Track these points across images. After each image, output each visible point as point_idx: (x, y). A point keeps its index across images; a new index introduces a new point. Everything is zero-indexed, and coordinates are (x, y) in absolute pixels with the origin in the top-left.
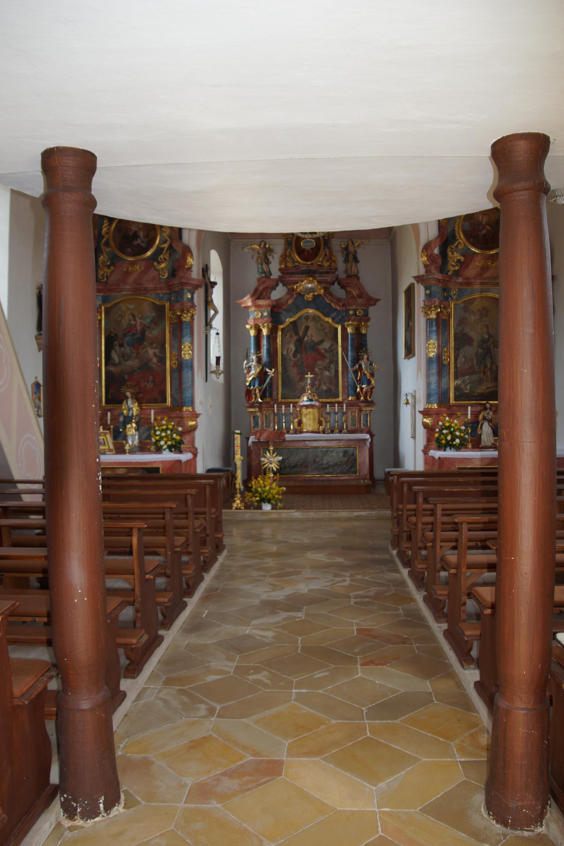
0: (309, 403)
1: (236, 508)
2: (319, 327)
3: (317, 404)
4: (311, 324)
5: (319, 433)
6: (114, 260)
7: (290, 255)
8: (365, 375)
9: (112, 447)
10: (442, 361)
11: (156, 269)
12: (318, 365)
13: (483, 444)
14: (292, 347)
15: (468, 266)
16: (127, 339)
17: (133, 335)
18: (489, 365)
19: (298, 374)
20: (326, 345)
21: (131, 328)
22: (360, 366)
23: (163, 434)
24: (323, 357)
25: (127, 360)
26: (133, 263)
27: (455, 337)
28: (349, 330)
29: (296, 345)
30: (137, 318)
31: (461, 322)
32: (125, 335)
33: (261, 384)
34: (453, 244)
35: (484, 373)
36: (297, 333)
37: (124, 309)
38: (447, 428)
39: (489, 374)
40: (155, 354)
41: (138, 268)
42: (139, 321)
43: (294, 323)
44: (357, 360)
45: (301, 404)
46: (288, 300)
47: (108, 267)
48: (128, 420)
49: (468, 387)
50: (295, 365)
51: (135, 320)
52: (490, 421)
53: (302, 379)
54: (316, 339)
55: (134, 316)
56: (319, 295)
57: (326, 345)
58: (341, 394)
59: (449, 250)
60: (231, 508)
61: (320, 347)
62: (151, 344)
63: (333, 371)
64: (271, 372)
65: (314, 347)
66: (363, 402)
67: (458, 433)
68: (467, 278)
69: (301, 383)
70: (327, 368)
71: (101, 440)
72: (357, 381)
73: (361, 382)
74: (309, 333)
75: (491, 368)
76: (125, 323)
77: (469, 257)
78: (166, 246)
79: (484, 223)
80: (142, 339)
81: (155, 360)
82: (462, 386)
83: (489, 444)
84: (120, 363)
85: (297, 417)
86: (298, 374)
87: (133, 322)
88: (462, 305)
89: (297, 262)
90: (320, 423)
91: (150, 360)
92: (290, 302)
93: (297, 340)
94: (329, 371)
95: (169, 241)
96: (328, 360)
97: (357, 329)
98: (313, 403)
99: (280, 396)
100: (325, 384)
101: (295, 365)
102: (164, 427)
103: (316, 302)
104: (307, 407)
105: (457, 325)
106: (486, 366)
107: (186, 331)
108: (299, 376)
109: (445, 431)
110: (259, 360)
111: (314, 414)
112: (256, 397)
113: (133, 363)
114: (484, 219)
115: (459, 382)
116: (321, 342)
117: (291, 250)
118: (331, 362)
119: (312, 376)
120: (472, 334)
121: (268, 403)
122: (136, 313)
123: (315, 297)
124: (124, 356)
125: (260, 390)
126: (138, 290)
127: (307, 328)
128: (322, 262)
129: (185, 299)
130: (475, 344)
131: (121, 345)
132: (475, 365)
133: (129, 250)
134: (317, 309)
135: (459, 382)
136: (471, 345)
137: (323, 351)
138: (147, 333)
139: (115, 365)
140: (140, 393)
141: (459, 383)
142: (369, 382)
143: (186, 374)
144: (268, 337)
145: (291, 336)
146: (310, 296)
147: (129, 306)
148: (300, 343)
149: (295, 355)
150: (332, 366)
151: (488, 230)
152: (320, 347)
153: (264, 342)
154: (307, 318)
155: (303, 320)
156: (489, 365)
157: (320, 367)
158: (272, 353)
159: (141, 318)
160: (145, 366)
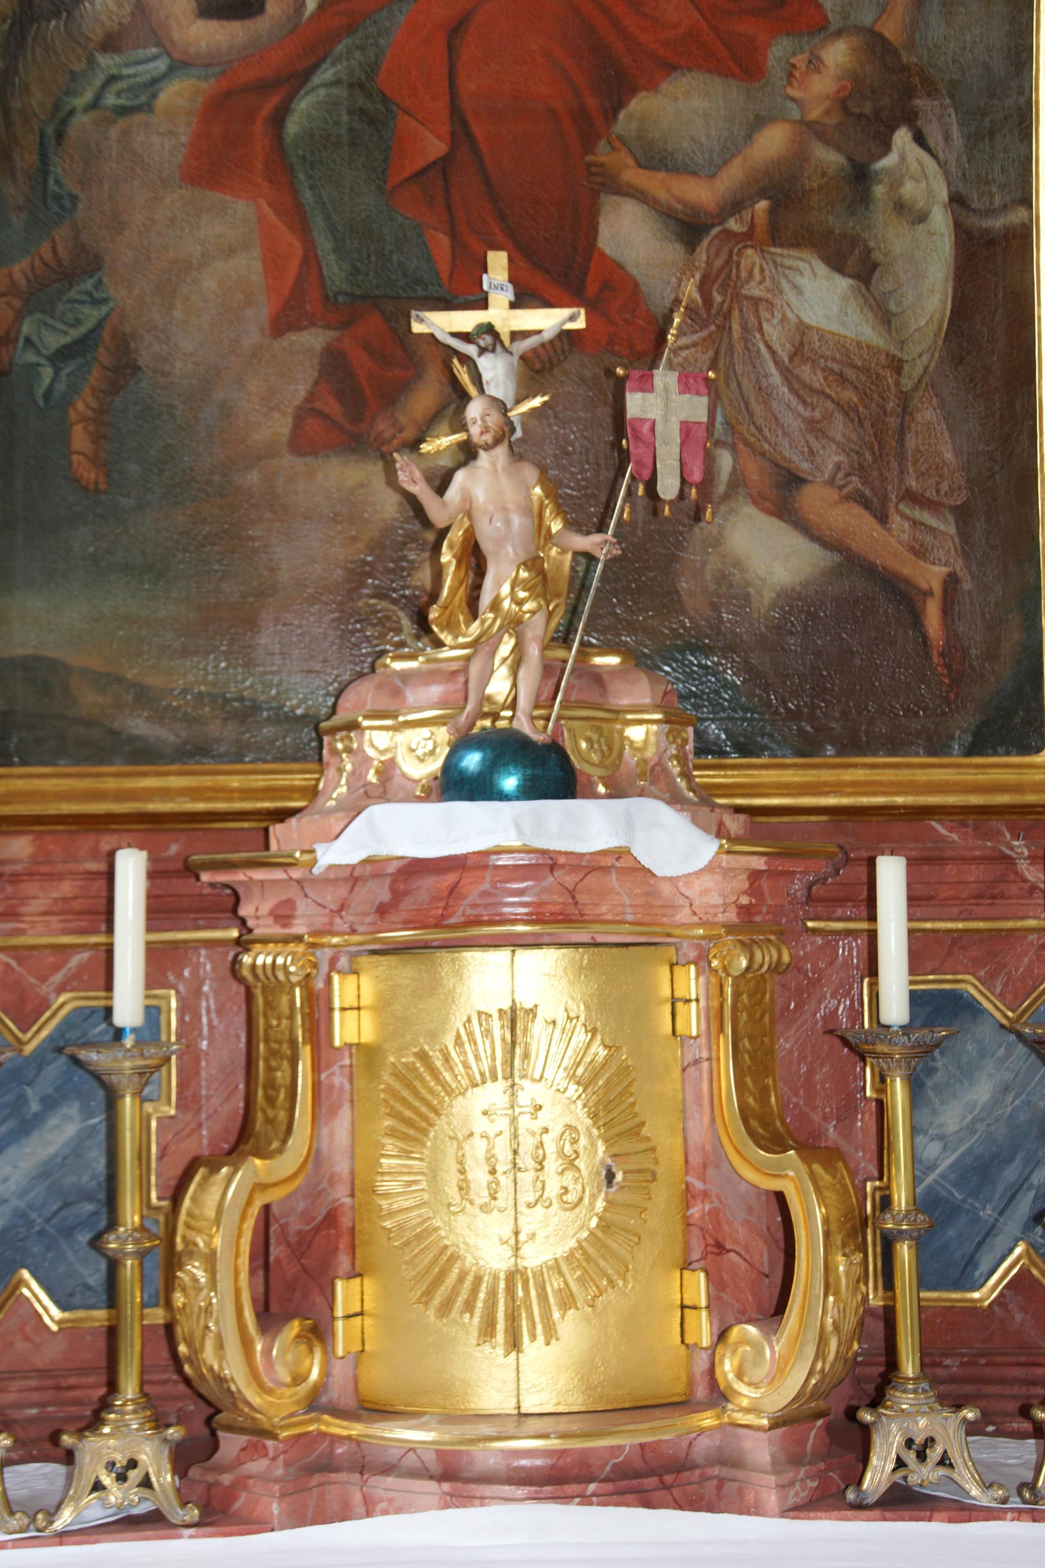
3: (676, 846)
12: (656, 158)
19: (281, 324)
45: (338, 853)
69: (344, 475)
70: (818, 212)
86: (281, 324)
94: (857, 262)
96: (837, 54)
100: (783, 494)
104: (433, 910)
108: (314, 340)
111: (613, 1100)
118: (887, 97)
119: (546, 321)
150: (913, 167)
157: (701, 193)
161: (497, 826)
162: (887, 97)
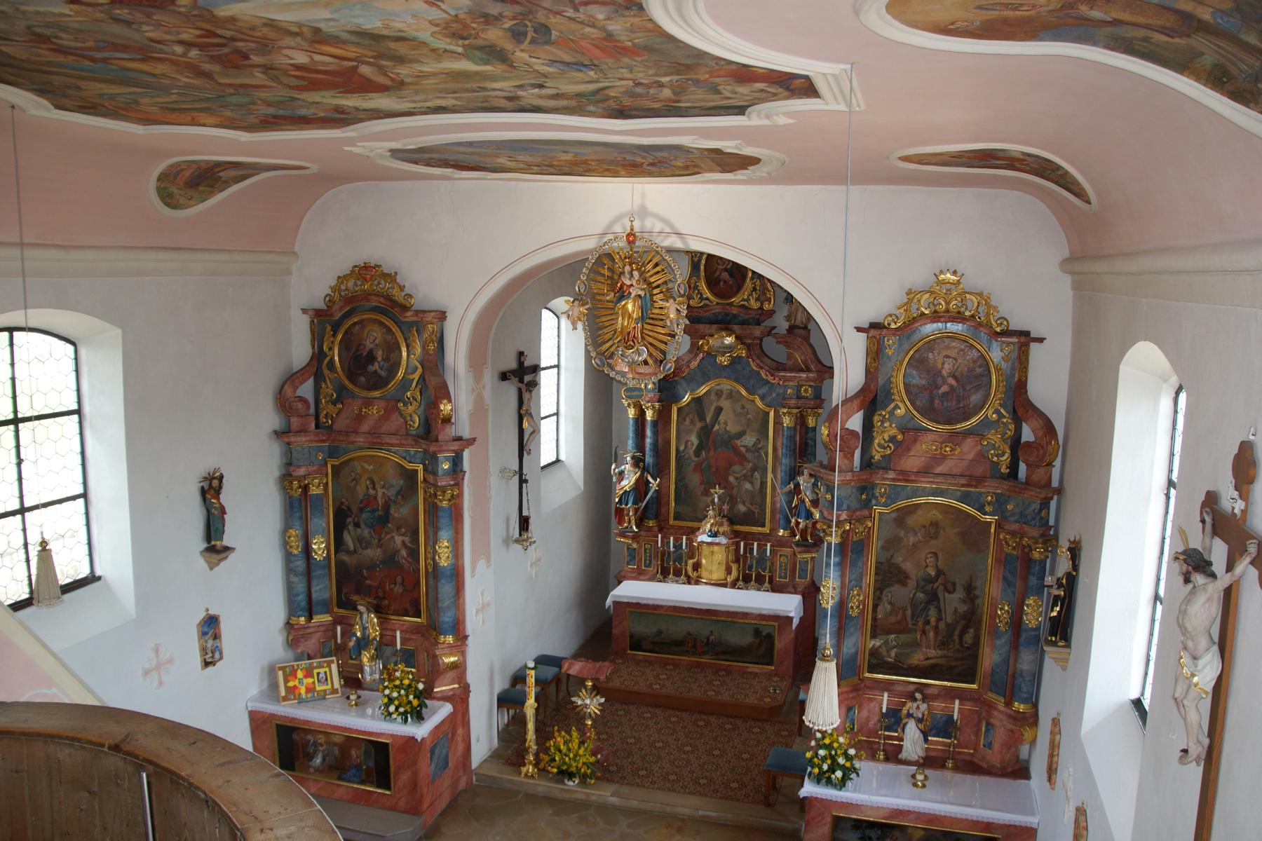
0: (709, 540)
1: (526, 775)
2: (739, 410)
4: (725, 404)
5: (724, 585)
6: (342, 395)
7: (696, 287)
8: (803, 501)
9: (337, 685)
10: (847, 611)
11: (401, 415)
13: (903, 755)
14: (694, 440)
15: (908, 449)
16: (364, 516)
17: (373, 511)
18: (933, 620)
20: (749, 440)
21: (369, 501)
22: (797, 485)
23: (395, 694)
24: (742, 459)
25: (366, 548)
26: (368, 403)
27: (877, 568)
28: (787, 421)
29: (699, 437)
30: (377, 486)
31: (891, 544)
32: (361, 510)
33: (635, 503)
34: (884, 409)
35: (924, 632)
36: (702, 418)
37: (359, 469)
38: (829, 747)
39: (932, 634)
40: (403, 542)
41: (375, 411)
42: (380, 492)
43: (698, 401)
44: (794, 473)
46: (689, 362)
47: (334, 403)
48: (363, 643)
49: (893, 653)
50: (698, 467)
51: (374, 488)
52: (919, 721)
53: (706, 493)
54: (733, 428)
55: (373, 482)
56: (739, 357)
57: (749, 440)
58: (768, 520)
59: (876, 418)
60: (520, 773)
61: (739, 442)
62: (398, 529)
63: (758, 486)
64: (654, 484)
65: (729, 441)
66: (798, 544)
67: (841, 761)
68: (903, 473)
70: (749, 478)
71: (322, 675)
72: (791, 510)
73: (795, 511)
74: (722, 418)
75: (937, 627)
76: (361, 491)
77: (911, 432)
78: (416, 376)
79: (944, 373)
80: (385, 518)
81: (404, 553)
82: (883, 651)
83: (914, 757)
84: (355, 551)
85: (692, 557)
87: (372, 492)
88: (894, 515)
89: (707, 299)
90: (729, 571)
91: (398, 551)
92: (694, 364)
93: (702, 428)
94: (752, 483)
95: (420, 371)
97: (801, 420)
98: (717, 540)
99: (672, 515)
100: (744, 503)
101: (698, 467)
102: (398, 682)
103: (735, 369)
105: (883, 548)
106: (927, 622)
107: (444, 521)
109: (822, 752)
110: (637, 462)
112: (630, 522)
113: (374, 553)
114: (947, 366)
115: (877, 643)
116: (741, 435)
117: (699, 278)
118: (754, 469)
120: (907, 566)
121: (649, 529)
122: (376, 479)
123: (735, 361)
124: (360, 540)
125: (636, 510)
126: (376, 440)
127: (719, 410)
128: (748, 300)
129: (440, 472)
130: (912, 583)
131: (357, 525)
132: (909, 618)
133: (363, 379)
134: (737, 381)
135: (877, 643)
136: (904, 584)
137: (743, 449)
138: (392, 511)
139: (348, 552)
140: (385, 598)
141: (878, 644)
142: (809, 515)
143: (446, 589)
144: (655, 424)
145: (692, 422)
146: (724, 360)
147: (366, 466)
148: (705, 433)
149: (697, 453)
151: (951, 386)
152: (739, 442)
153: (649, 432)
154: (719, 394)
155: (713, 397)
156: (933, 620)
158: (661, 451)
159: (383, 487)
160: (391, 559)
161: (709, 540)
162: (754, 469)
